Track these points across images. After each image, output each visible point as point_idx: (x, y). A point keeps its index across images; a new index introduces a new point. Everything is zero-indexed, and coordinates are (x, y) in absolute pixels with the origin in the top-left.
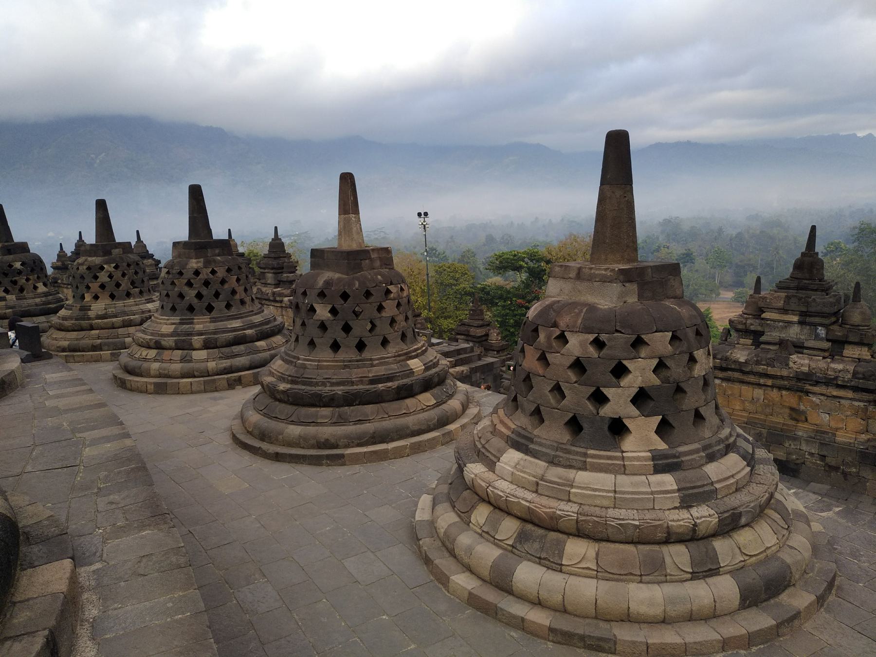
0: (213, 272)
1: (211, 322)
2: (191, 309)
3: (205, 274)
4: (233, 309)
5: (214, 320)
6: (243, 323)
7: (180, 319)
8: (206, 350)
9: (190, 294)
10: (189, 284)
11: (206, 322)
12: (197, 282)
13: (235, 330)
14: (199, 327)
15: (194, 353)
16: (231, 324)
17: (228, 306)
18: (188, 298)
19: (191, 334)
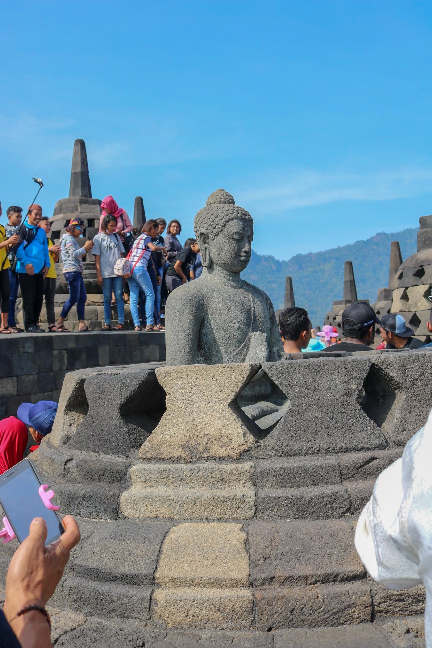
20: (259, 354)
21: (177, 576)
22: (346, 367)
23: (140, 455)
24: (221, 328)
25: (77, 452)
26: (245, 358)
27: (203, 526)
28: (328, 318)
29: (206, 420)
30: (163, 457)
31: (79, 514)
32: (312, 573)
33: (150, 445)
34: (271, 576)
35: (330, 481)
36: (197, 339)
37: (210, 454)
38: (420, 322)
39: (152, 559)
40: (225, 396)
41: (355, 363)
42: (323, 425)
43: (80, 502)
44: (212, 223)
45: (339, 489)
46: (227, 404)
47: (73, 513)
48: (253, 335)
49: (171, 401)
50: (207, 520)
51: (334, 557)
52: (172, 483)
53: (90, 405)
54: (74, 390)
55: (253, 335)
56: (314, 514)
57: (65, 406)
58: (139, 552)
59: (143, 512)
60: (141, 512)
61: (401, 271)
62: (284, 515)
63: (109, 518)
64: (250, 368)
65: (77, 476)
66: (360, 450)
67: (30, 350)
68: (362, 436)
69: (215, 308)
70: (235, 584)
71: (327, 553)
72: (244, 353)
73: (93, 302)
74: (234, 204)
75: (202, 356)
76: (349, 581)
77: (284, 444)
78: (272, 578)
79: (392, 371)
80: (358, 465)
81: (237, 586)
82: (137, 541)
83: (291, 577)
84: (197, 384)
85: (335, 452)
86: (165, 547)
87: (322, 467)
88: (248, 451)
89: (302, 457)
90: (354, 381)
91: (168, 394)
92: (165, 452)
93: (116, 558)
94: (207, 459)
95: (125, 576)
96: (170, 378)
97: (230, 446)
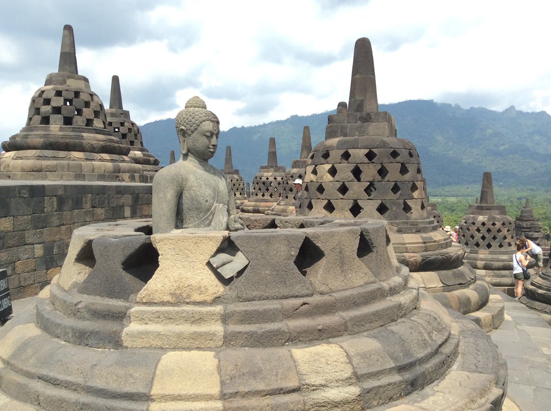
0: (494, 224)
1: (489, 254)
2: (477, 245)
3: (489, 225)
4: (503, 248)
5: (491, 253)
6: (509, 257)
7: (470, 250)
8: (484, 270)
9: (478, 236)
10: (478, 230)
11: (486, 253)
12: (483, 230)
13: (503, 261)
14: (481, 256)
15: (477, 270)
16: (501, 257)
17: (501, 246)
18: (476, 238)
19: (476, 259)
20: (222, 220)
21: (167, 393)
22: (288, 240)
23: (138, 300)
24: (194, 200)
25: (85, 296)
26: (211, 222)
27: (185, 354)
28: (256, 178)
29: (189, 274)
30: (155, 301)
31: (88, 345)
32: (265, 388)
33: (145, 293)
34: (236, 392)
35: (275, 320)
36: (176, 208)
37: (191, 300)
38: (324, 190)
39: (148, 381)
40: (204, 257)
41: (294, 237)
42: (271, 280)
43: (89, 336)
44: (189, 122)
45: (282, 326)
46: (205, 264)
47: (82, 344)
48: (217, 206)
49: (163, 261)
50: (189, 349)
51: (279, 376)
52: (162, 321)
53: (97, 261)
54: (83, 247)
55: (217, 206)
56: (264, 344)
57: (74, 259)
58: (138, 375)
59: (139, 343)
60: (138, 343)
61: (313, 153)
62: (244, 345)
63: (112, 348)
64: (222, 238)
65: (86, 315)
66: (296, 297)
67: (25, 196)
68: (297, 287)
69: (191, 186)
70: (209, 398)
71: (274, 373)
72: (210, 218)
73: (78, 158)
74: (206, 108)
75: (179, 220)
76: (289, 393)
77: (245, 293)
78: (237, 393)
79: (318, 243)
80: (295, 309)
81: (211, 399)
82: (136, 367)
83: (250, 392)
84: (182, 249)
85: (278, 298)
86: (158, 372)
87: (270, 310)
88: (218, 297)
89: (256, 302)
90: (293, 249)
91: (160, 255)
92: (157, 298)
93: (120, 380)
94: (188, 303)
95: (127, 394)
96: (162, 244)
97: (206, 294)
